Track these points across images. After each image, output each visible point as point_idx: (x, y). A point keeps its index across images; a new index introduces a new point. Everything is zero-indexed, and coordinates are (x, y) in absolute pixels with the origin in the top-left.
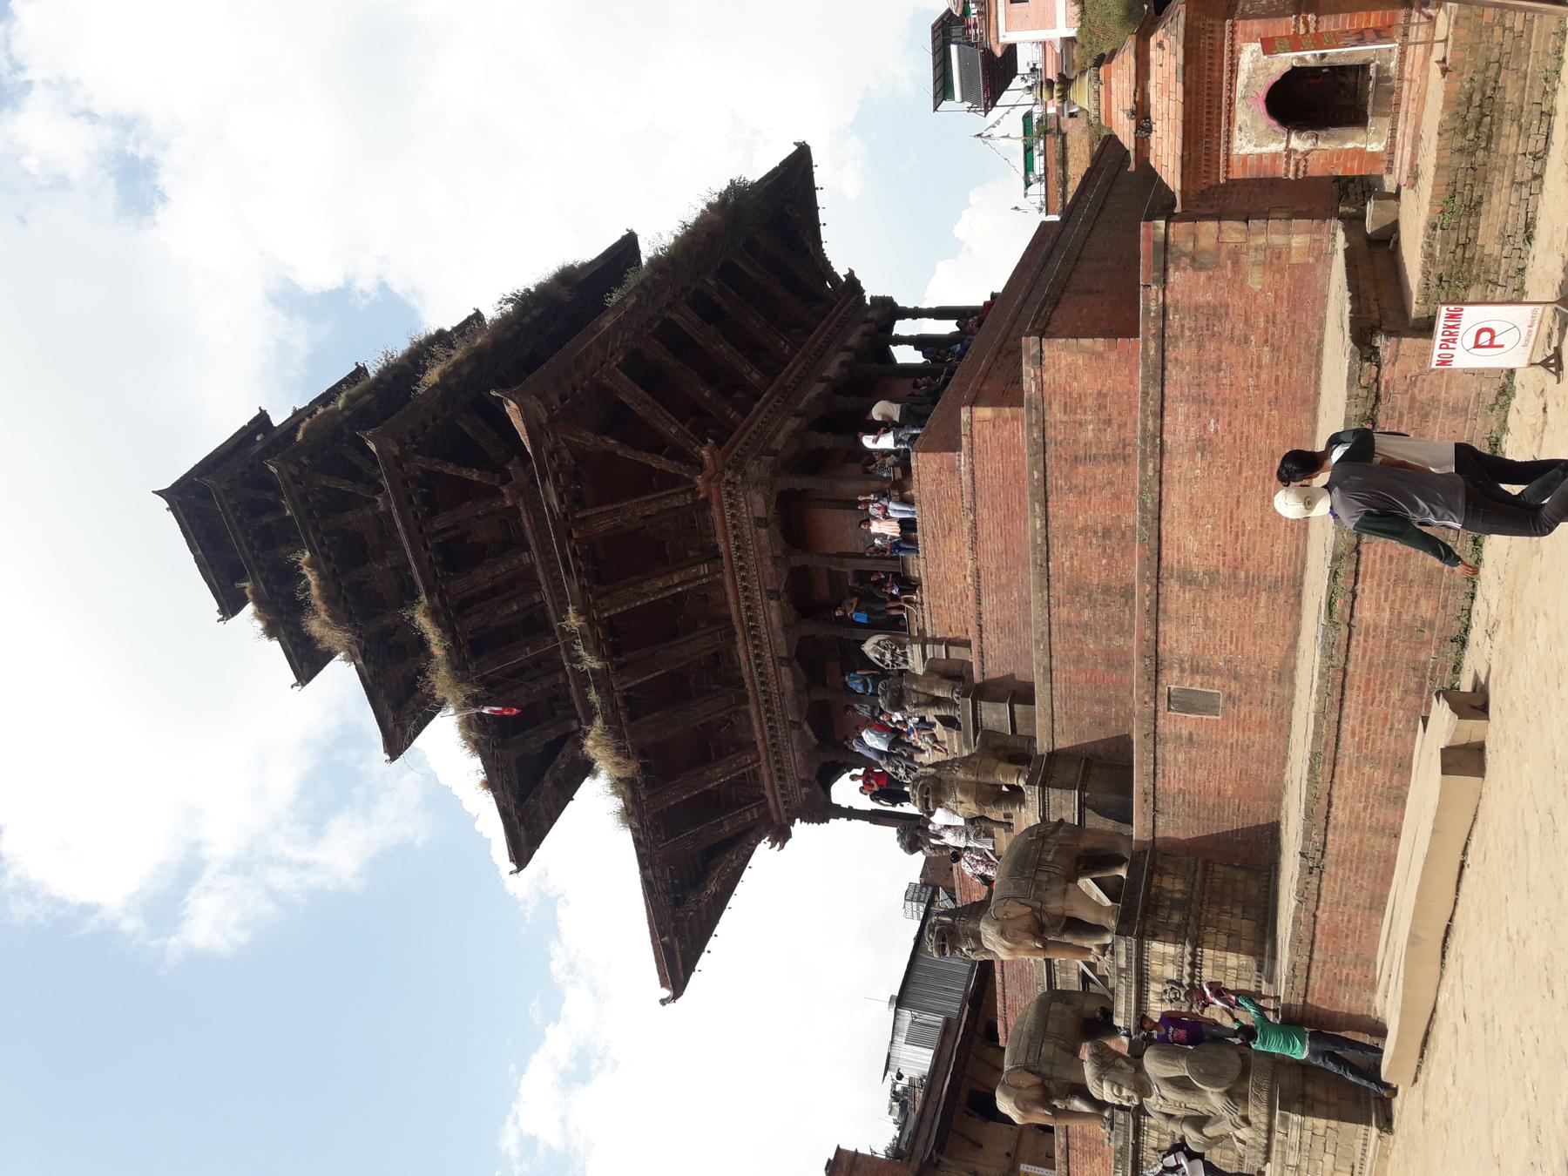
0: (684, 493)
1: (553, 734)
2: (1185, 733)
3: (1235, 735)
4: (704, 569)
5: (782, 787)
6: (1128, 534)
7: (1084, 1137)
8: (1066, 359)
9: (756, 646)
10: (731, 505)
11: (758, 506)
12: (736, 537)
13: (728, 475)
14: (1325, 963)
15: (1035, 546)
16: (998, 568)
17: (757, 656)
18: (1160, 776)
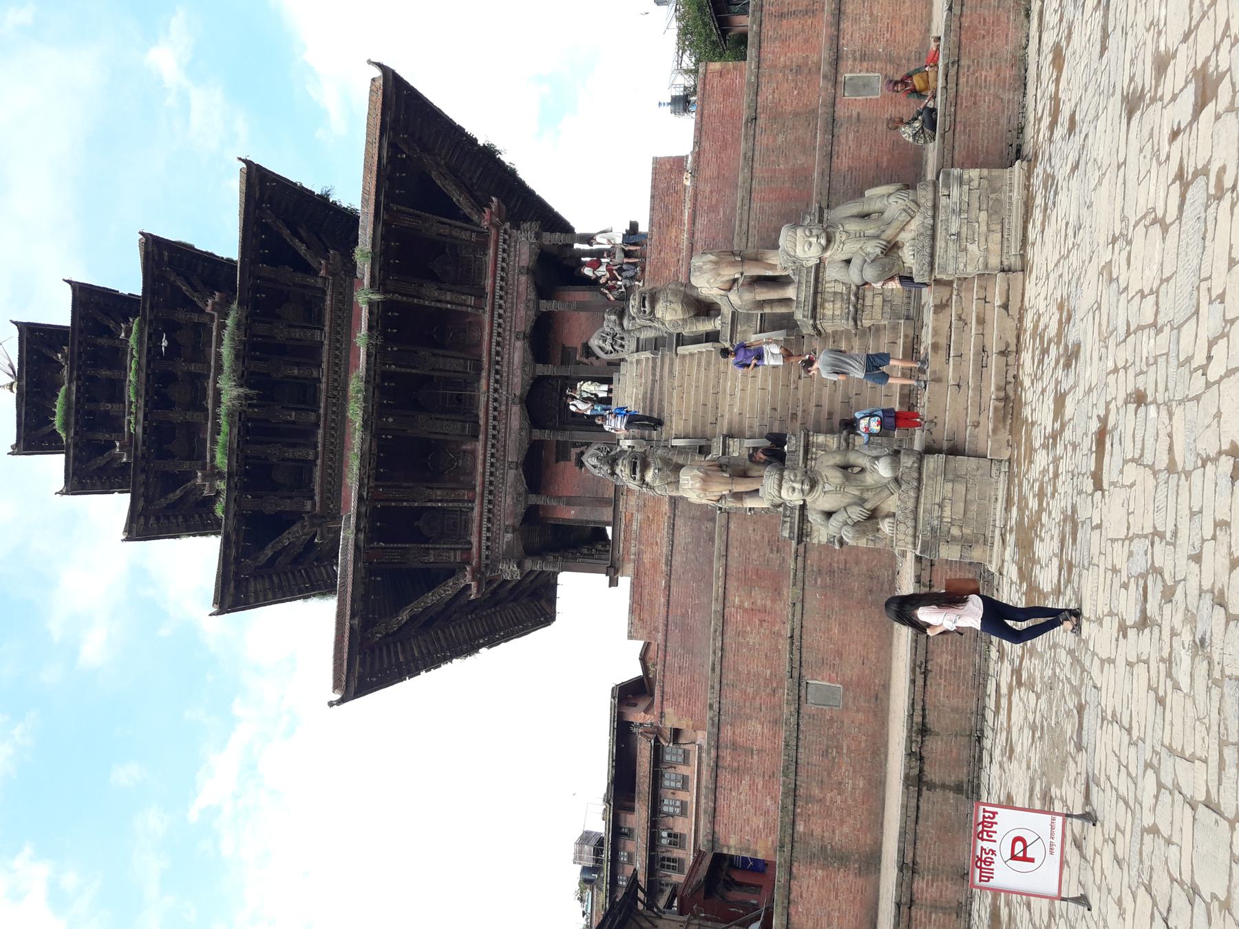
0: (472, 231)
1: (287, 505)
2: (855, 114)
4: (471, 300)
5: (488, 530)
6: (814, 69)
9: (497, 381)
10: (504, 250)
11: (523, 257)
12: (502, 279)
13: (508, 225)
14: (969, 67)
15: (749, 83)
16: (711, 192)
17: (496, 390)
18: (835, 157)
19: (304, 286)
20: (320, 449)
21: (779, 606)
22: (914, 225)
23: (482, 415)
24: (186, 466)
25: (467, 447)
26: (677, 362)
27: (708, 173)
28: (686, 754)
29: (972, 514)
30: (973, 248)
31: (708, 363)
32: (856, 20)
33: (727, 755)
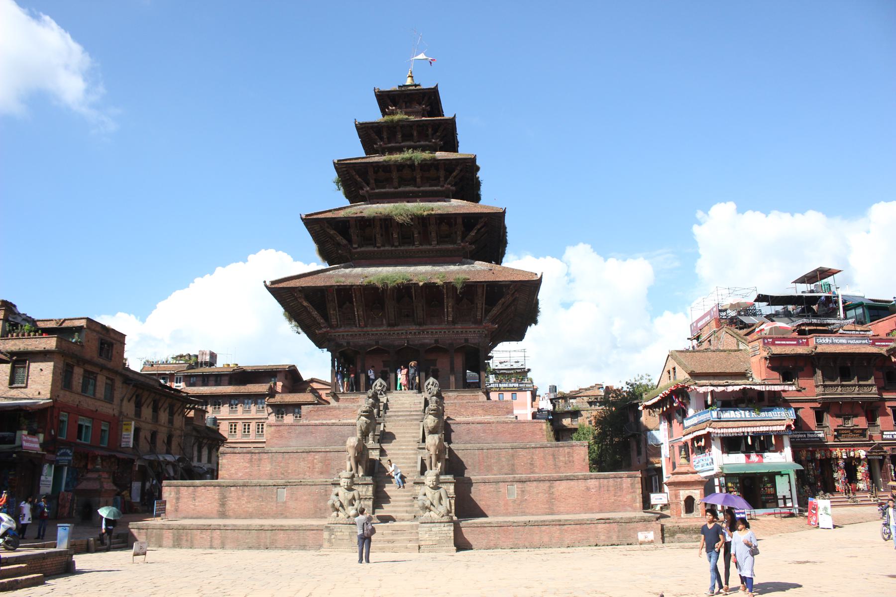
3: (502, 503)
4: (450, 319)
7: (260, 460)
8: (582, 452)
19: (456, 233)
20: (382, 249)
21: (316, 474)
22: (436, 516)
23: (399, 328)
24: (372, 181)
25: (384, 322)
26: (418, 422)
27: (499, 428)
28: (263, 411)
29: (339, 542)
30: (427, 536)
31: (414, 437)
32: (537, 487)
33: (256, 457)
